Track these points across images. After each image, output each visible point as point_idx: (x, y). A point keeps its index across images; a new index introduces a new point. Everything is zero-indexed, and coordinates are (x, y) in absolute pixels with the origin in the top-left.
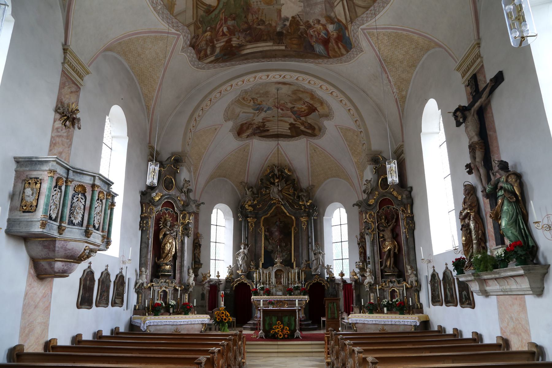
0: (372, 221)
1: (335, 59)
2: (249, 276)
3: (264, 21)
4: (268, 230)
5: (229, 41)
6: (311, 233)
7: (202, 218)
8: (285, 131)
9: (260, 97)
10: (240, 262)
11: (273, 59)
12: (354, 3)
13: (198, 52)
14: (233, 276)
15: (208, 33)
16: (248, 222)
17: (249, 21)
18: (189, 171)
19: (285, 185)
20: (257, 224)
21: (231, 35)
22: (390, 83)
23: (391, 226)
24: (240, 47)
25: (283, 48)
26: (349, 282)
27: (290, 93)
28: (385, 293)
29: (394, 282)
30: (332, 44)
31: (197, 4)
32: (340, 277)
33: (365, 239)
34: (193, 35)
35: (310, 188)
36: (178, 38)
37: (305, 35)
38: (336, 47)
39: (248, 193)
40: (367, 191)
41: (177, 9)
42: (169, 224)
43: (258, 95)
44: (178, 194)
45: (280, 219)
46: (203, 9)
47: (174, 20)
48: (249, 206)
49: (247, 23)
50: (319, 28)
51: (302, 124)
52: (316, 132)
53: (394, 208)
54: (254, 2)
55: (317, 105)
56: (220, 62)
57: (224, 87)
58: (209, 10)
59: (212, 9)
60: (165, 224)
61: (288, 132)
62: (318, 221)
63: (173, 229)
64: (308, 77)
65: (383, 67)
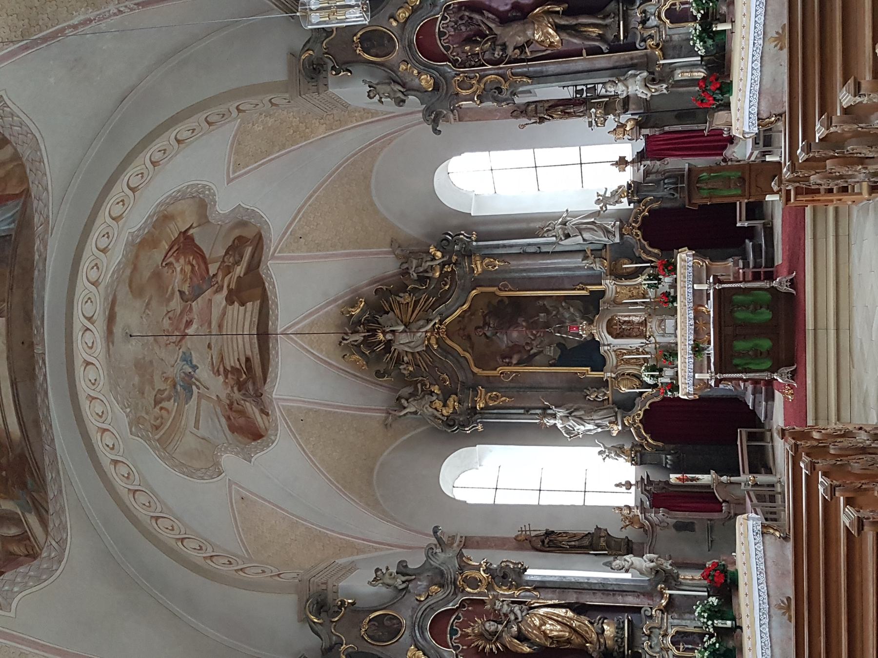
0: (479, 82)
2: (625, 405)
4: (506, 357)
6: (511, 246)
7: (477, 530)
8: (248, 315)
9: (152, 382)
10: (591, 427)
11: (38, 350)
14: (627, 447)
16: (487, 407)
18: (351, 568)
19: (391, 314)
20: (491, 384)
22: (91, 21)
23: (492, 26)
26: (641, 144)
27: (139, 304)
28: (675, 38)
29: (644, 12)
32: (629, 168)
33: (528, 104)
35: (398, 252)
39: (413, 409)
40: (400, 95)
42: (491, 626)
43: (147, 388)
44: (410, 600)
45: (477, 328)
48: (445, 405)
51: (228, 270)
52: (249, 233)
53: (444, 18)
55: (173, 231)
57: (120, 484)
60: (495, 636)
61: (253, 307)
62: (482, 228)
63: (506, 615)
64: (86, 254)
65: (45, 39)
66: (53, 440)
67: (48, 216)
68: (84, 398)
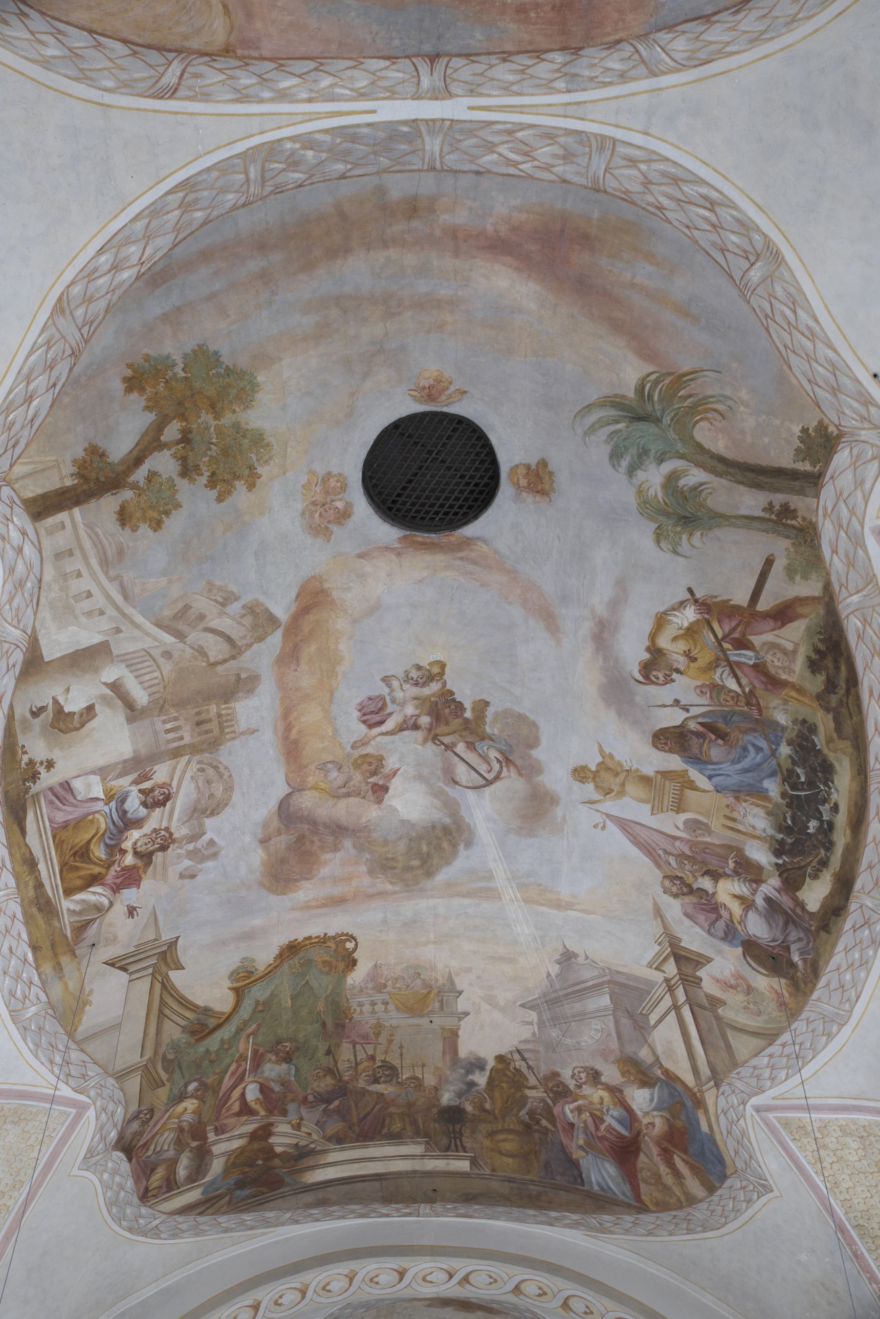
1: (666, 1216)
3: (393, 1068)
5: (264, 1133)
11: (424, 1208)
12: (718, 1018)
13: (144, 1170)
15: (190, 1104)
17: (342, 1066)
21: (270, 1112)
24: (302, 1155)
25: (464, 1165)
30: (650, 1158)
31: (162, 1002)
34: (133, 1108)
36: (78, 1117)
37: (544, 1122)
38: (663, 1169)
41: (89, 1020)
46: (183, 1023)
47: (75, 1055)
49: (331, 1071)
50: (596, 1098)
54: (361, 1005)
56: (218, 1212)
58: (203, 1025)
59: (212, 1022)
66: (297, 1222)
67: (612, 1233)
68: (352, 1267)
